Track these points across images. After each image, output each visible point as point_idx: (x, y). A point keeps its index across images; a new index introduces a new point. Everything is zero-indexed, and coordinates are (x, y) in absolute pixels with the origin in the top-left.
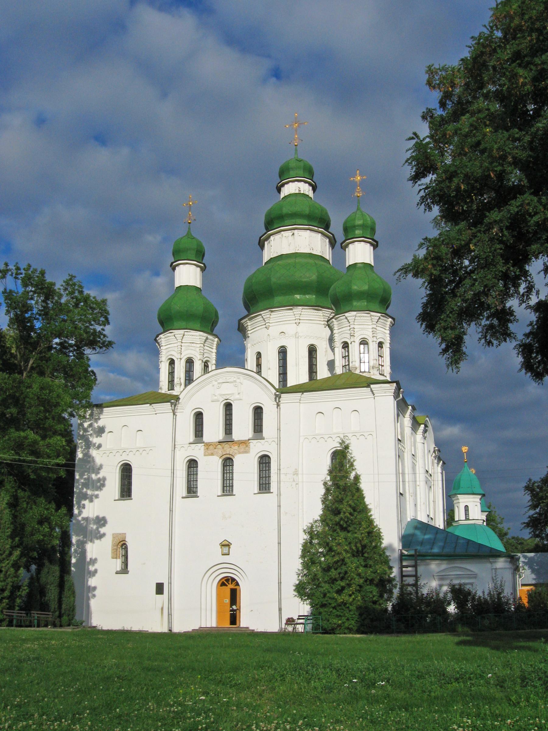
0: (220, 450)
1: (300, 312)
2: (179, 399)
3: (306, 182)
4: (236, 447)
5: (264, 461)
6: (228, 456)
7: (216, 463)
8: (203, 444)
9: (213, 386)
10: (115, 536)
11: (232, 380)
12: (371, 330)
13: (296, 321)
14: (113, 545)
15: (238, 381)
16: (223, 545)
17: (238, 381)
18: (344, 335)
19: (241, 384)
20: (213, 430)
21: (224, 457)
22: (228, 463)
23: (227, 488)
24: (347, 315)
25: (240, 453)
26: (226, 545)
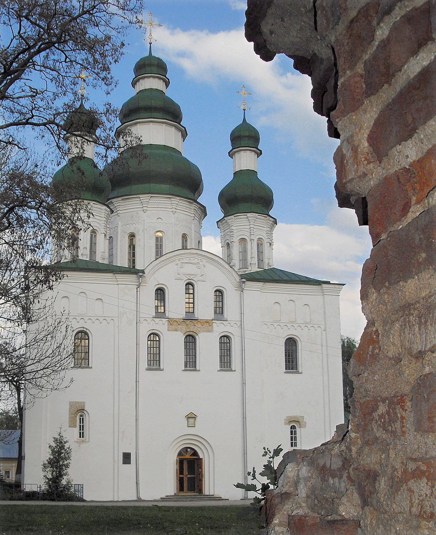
0: (184, 328)
1: (177, 203)
2: (144, 273)
3: (164, 81)
4: (200, 325)
5: (225, 341)
6: (191, 333)
7: (179, 338)
8: (167, 320)
9: (177, 264)
10: (71, 404)
11: (196, 261)
12: (266, 232)
13: (173, 210)
14: (71, 413)
15: (201, 263)
16: (188, 418)
17: (201, 263)
18: (240, 232)
19: (204, 266)
20: (176, 306)
21: (187, 334)
22: (190, 341)
23: (191, 362)
24: (249, 215)
25: (204, 331)
26: (191, 417)
